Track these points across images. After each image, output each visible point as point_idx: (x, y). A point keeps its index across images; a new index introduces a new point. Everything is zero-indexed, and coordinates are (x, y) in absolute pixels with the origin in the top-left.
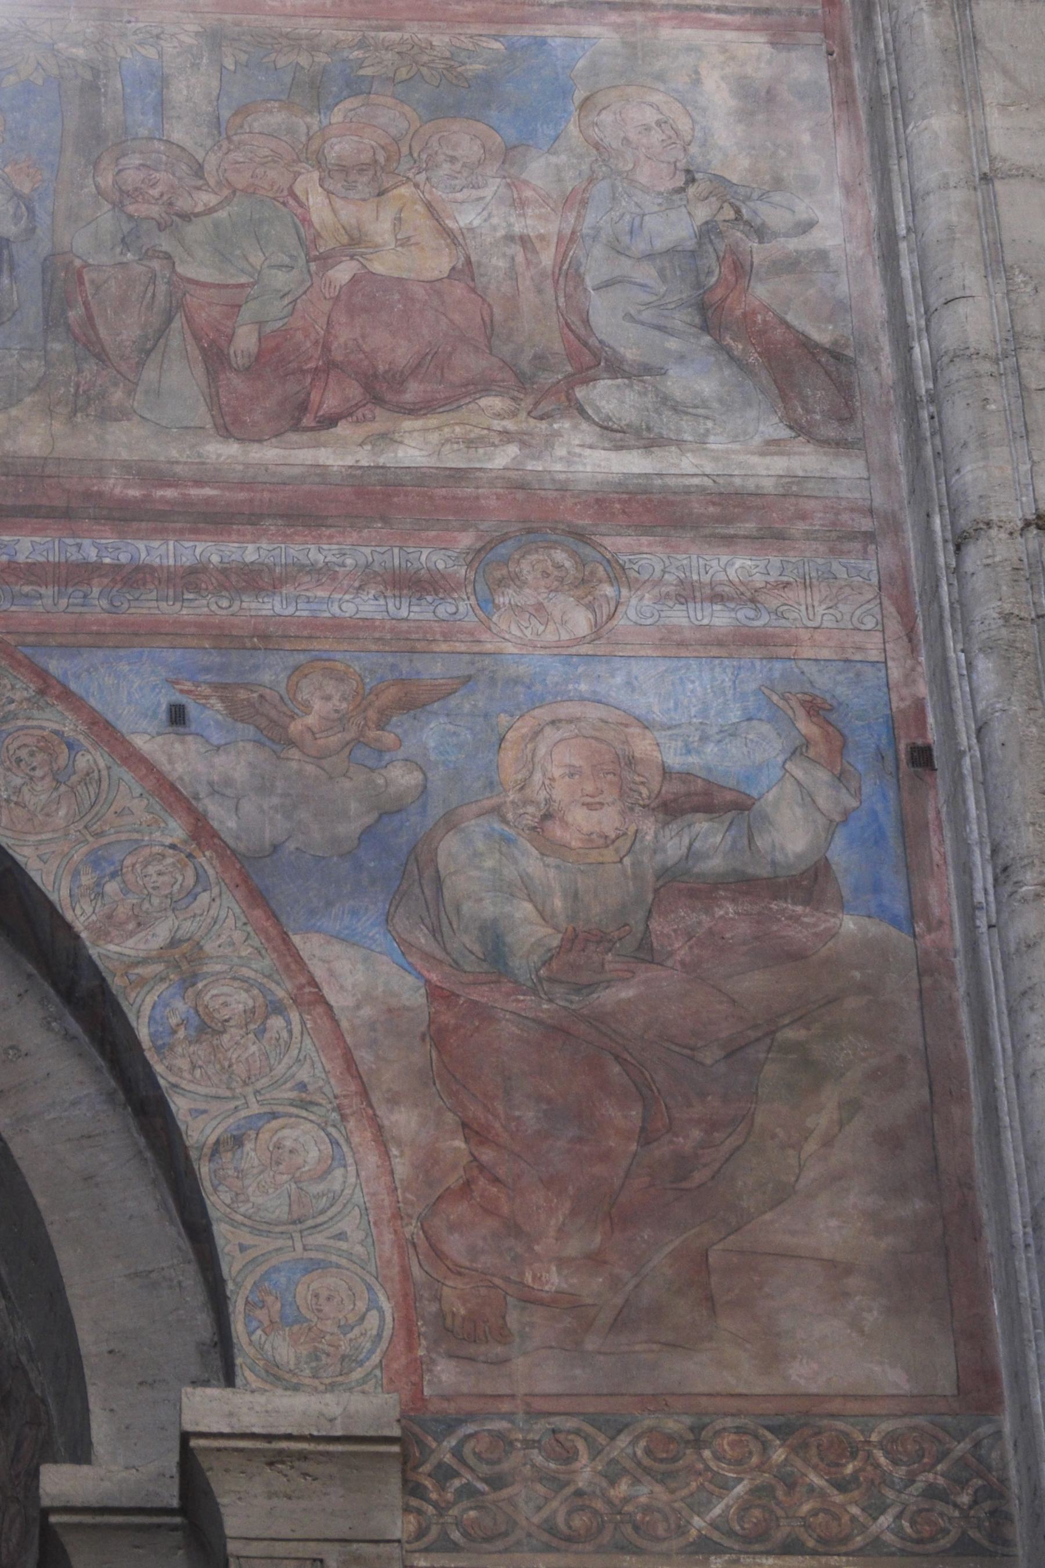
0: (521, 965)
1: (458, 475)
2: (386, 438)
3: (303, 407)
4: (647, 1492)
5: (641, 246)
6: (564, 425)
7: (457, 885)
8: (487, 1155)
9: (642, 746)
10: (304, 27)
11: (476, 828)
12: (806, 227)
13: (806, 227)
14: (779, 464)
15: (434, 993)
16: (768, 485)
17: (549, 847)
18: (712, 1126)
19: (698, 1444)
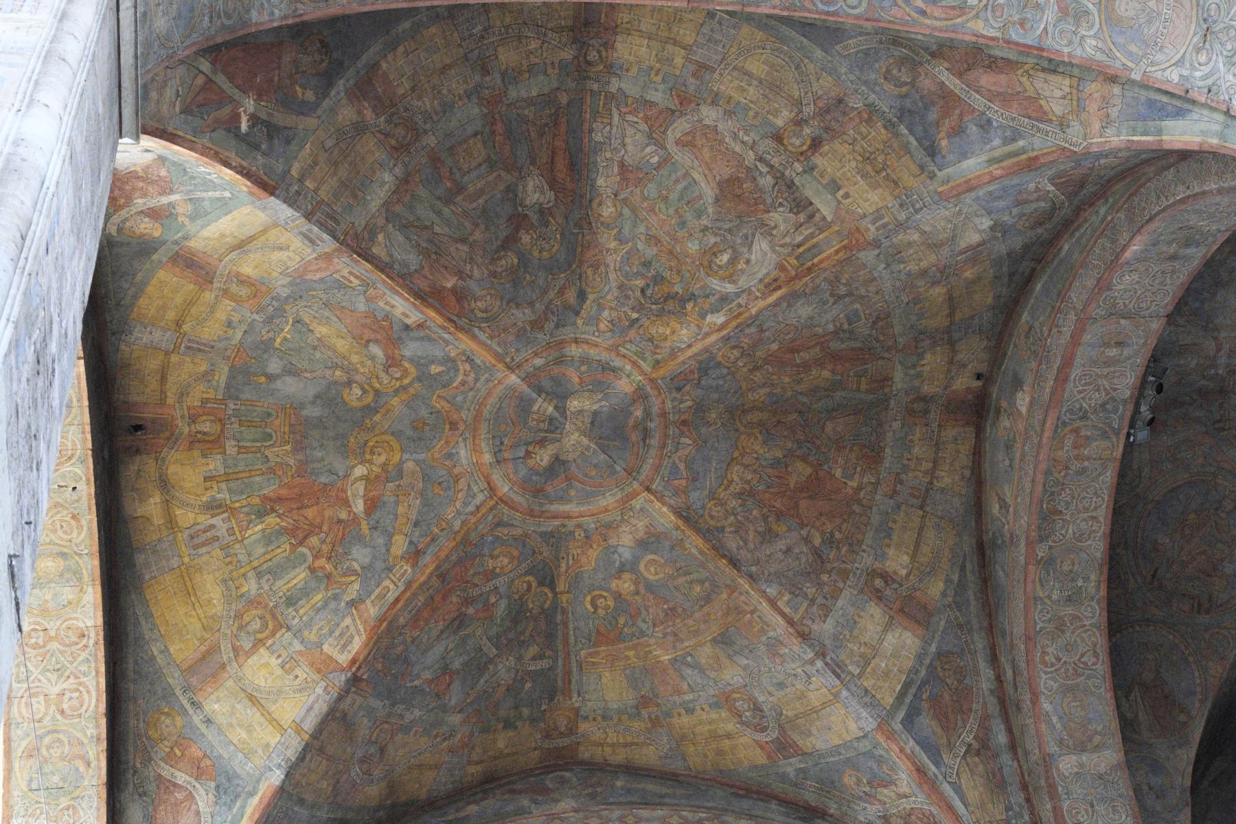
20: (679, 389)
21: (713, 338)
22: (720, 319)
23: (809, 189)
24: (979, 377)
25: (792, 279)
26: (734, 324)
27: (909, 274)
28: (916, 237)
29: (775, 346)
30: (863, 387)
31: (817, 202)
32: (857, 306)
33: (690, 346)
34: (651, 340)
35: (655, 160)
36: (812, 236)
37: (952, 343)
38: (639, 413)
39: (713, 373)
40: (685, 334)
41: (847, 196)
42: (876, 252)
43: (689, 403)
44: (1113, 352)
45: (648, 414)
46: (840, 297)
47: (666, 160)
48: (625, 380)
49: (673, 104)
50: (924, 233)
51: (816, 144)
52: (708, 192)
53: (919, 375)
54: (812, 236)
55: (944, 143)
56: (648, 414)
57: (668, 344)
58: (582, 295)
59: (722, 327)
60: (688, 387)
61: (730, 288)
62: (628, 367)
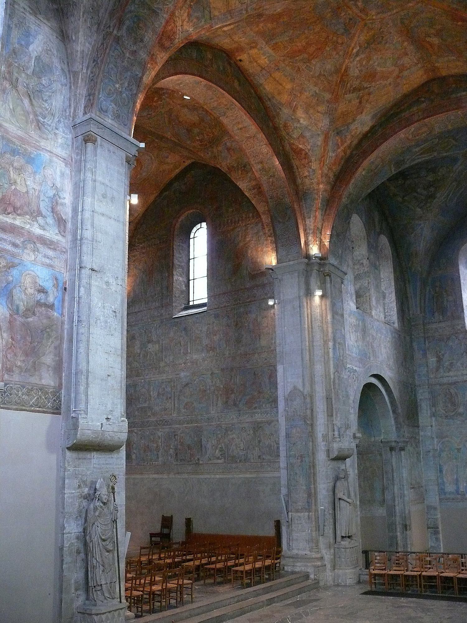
0: (21, 312)
1: (22, 228)
2: (14, 219)
3: (6, 210)
4: (26, 397)
5: (47, 195)
6: (35, 223)
7: (15, 298)
8: (13, 342)
9: (37, 281)
10: (14, 140)
11: (18, 288)
12: (65, 198)
13: (65, 198)
14: (57, 237)
15: (11, 315)
16: (55, 240)
17: (26, 294)
18: (38, 343)
19: (32, 391)
20: (350, 19)
21: (353, 45)
22: (355, 51)
23: (354, 94)
24: (240, 60)
25: (343, 75)
26: (350, 53)
27: (306, 91)
28: (320, 109)
29: (328, 49)
30: (280, 43)
31: (351, 95)
32: (311, 73)
33: (359, 37)
34: (372, 29)
35: (398, 62)
36: (346, 89)
37: (263, 69)
38: (359, 4)
39: (342, 31)
40: (362, 38)
41: (346, 103)
42: (326, 99)
43: (342, 15)
44: (240, 126)
45: (356, 5)
46: (320, 75)
47: (395, 65)
48: (374, 13)
49: (401, 75)
50: (318, 112)
51: (360, 102)
52: (378, 69)
53: (264, 54)
54: (346, 89)
55: (337, 138)
56: (356, 5)
57: (365, 32)
58: (402, 23)
59: (353, 49)
60: (347, 21)
61: (358, 59)
62: (374, 17)
